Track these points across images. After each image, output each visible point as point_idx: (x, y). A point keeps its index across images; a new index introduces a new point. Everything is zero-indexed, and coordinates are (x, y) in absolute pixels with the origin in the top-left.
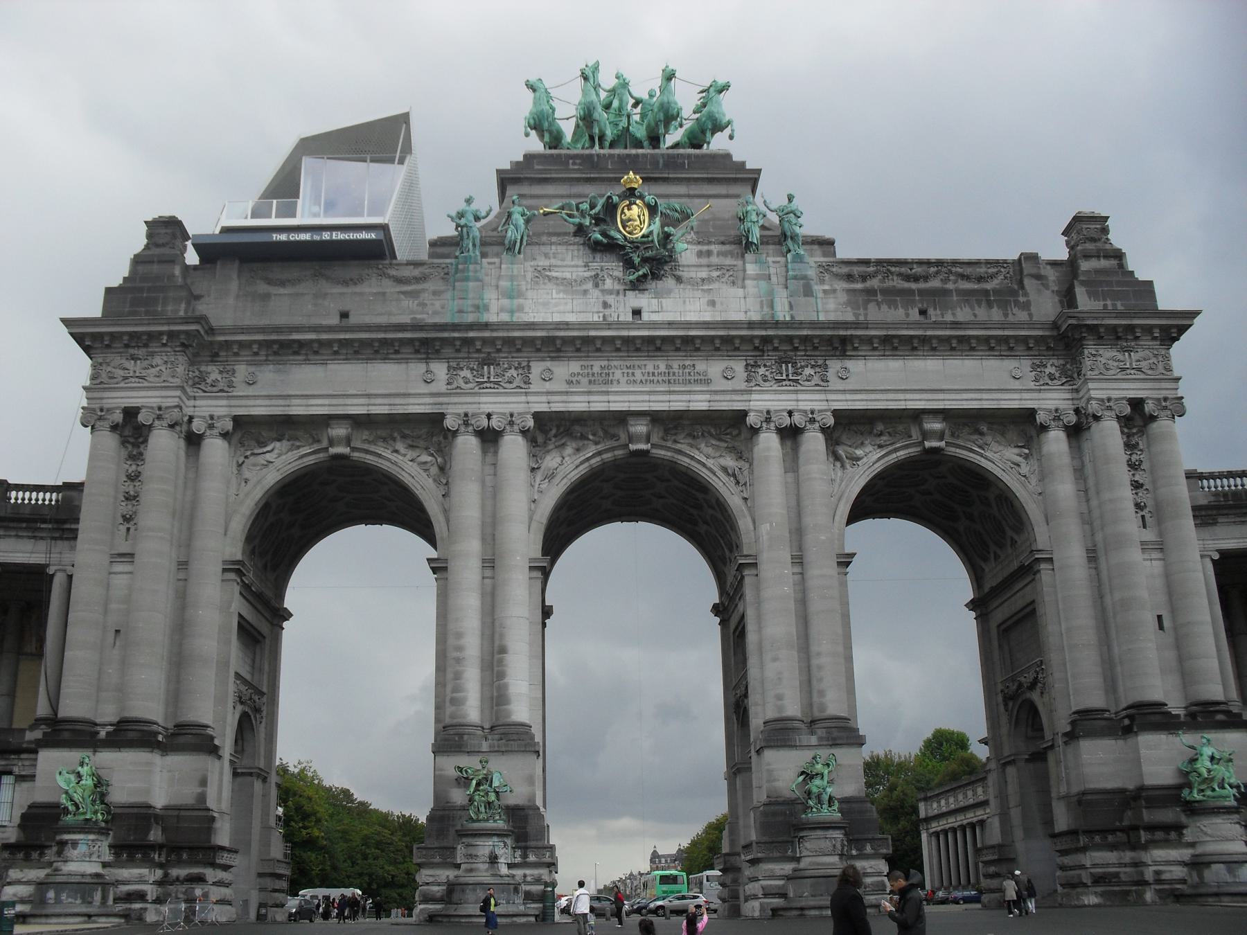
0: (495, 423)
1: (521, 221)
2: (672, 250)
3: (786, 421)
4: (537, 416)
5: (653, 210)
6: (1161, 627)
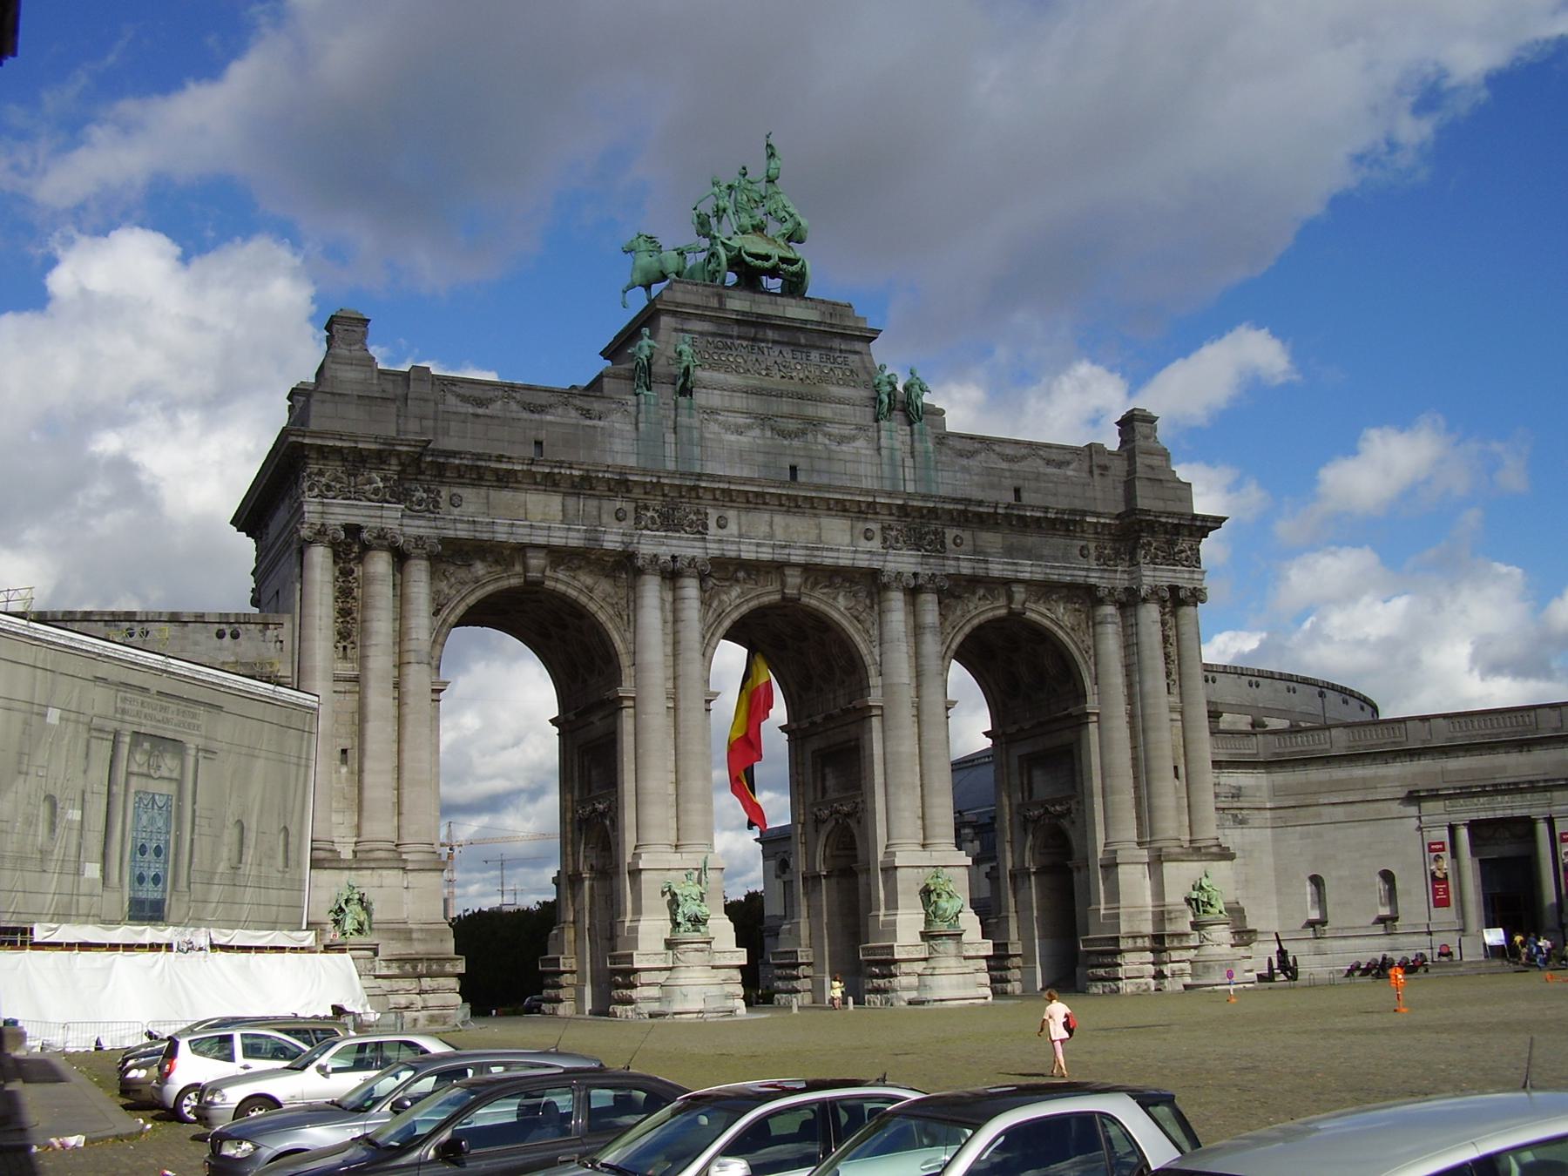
3: (912, 583)
6: (1177, 776)
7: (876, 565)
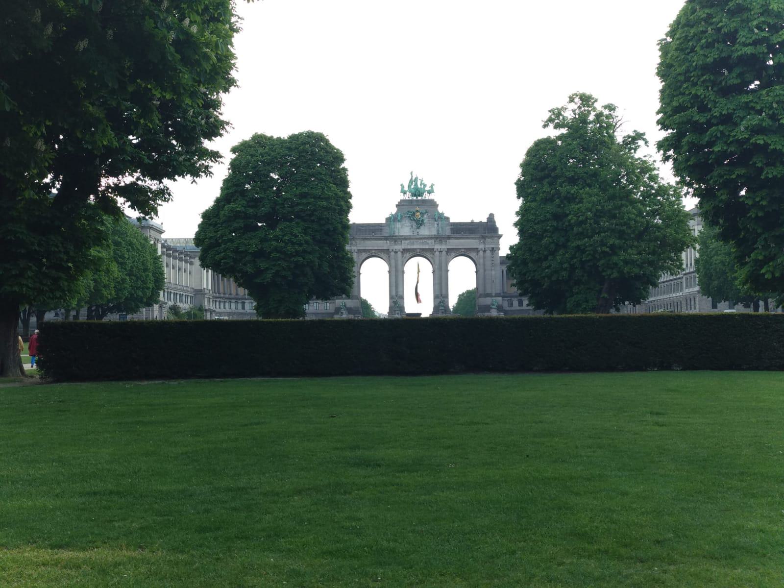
0: (397, 251)
1: (400, 216)
2: (423, 222)
4: (403, 249)
5: (421, 213)
7: (432, 247)
